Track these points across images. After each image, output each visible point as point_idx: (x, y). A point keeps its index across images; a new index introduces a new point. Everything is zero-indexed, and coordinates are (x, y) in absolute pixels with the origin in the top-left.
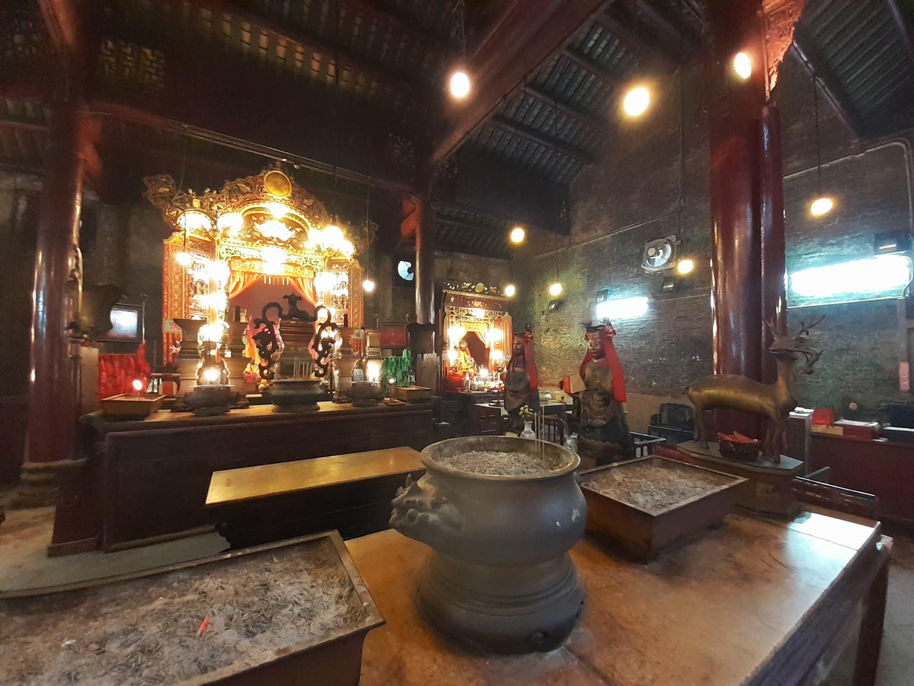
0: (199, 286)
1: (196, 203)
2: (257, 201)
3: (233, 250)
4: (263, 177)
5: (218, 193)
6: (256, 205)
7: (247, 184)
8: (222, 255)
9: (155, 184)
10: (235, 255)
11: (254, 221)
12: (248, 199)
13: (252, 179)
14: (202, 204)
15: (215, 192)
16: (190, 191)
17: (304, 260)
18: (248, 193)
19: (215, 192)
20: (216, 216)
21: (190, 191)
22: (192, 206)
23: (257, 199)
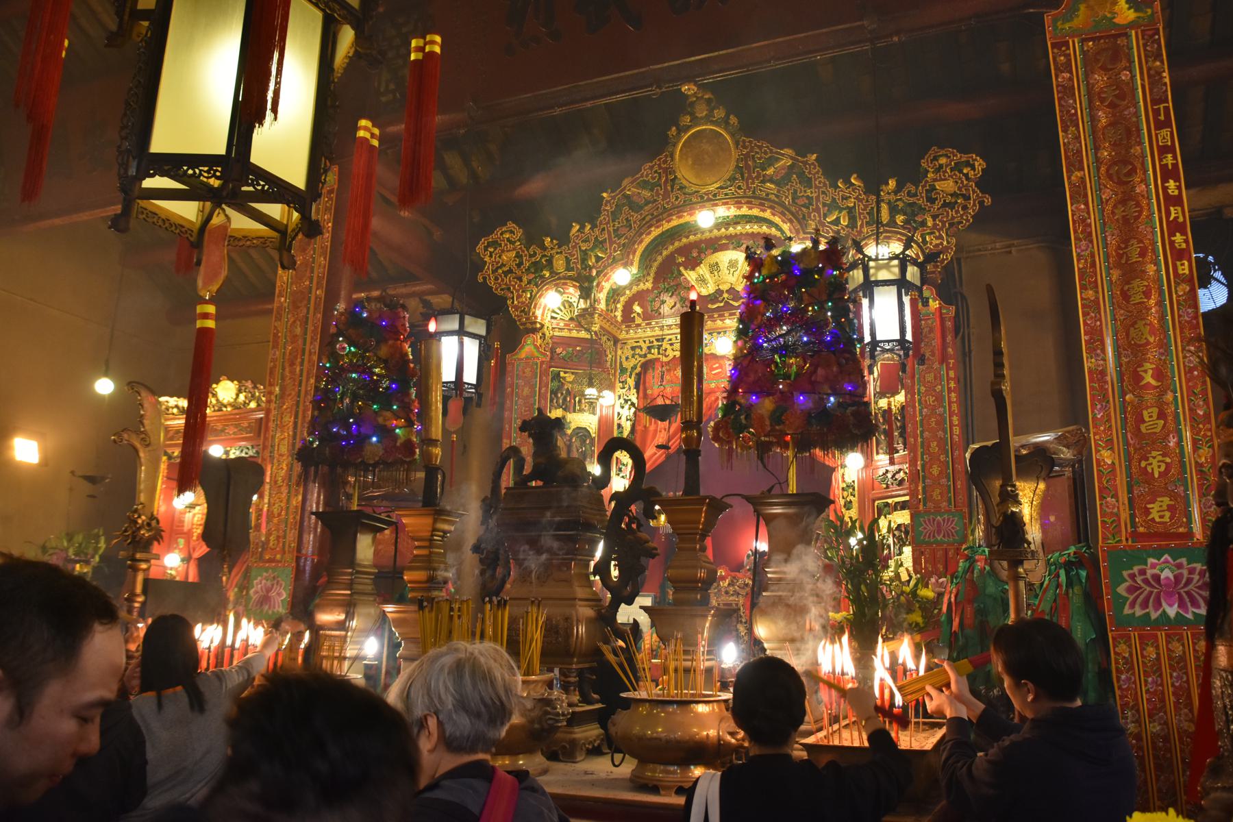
1: (559, 264)
3: (644, 346)
4: (672, 156)
7: (645, 185)
8: (625, 364)
9: (495, 249)
10: (650, 357)
12: (647, 219)
13: (651, 167)
14: (568, 261)
15: (588, 227)
18: (646, 204)
19: (588, 227)
22: (553, 273)
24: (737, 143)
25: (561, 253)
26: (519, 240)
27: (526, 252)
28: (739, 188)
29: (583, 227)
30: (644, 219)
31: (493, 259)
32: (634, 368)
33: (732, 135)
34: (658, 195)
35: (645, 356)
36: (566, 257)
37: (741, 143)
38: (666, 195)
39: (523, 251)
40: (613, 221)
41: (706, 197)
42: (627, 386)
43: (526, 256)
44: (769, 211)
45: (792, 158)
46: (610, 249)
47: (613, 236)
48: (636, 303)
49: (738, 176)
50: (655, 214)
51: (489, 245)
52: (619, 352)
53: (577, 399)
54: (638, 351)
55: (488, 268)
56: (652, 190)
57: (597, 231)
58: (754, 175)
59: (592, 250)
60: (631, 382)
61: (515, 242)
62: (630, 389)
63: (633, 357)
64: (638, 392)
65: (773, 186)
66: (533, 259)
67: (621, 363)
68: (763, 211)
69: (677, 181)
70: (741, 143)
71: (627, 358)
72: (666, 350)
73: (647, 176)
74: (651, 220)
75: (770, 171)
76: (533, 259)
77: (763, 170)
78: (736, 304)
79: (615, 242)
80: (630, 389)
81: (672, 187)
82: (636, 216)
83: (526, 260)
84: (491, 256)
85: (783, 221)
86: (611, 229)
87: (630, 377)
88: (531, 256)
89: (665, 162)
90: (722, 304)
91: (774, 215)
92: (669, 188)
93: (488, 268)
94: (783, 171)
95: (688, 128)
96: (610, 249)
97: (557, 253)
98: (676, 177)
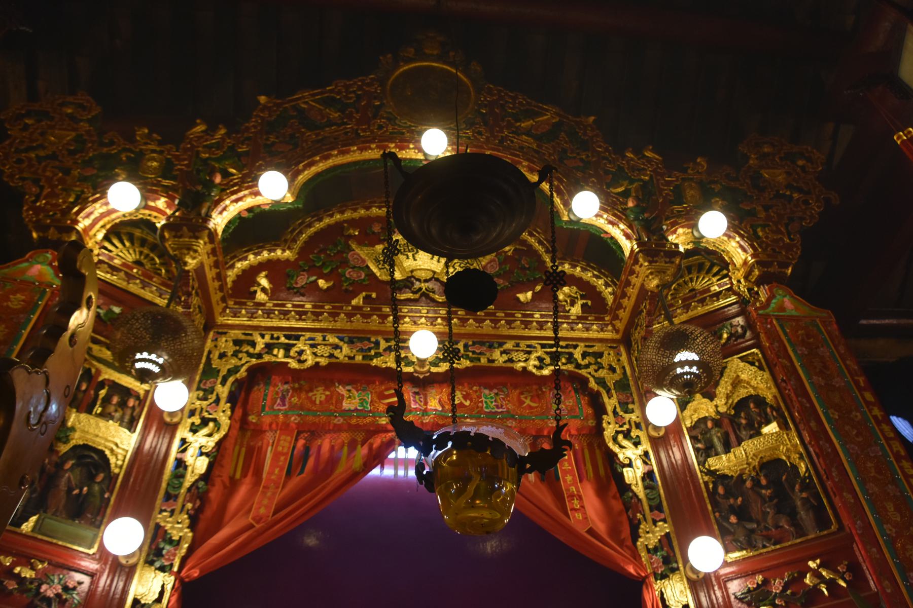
10: (267, 358)
11: (350, 237)
32: (235, 370)
35: (259, 356)
42: (213, 397)
48: (264, 274)
52: (209, 344)
53: (103, 393)
54: (246, 348)
60: (223, 391)
62: (217, 401)
63: (235, 354)
64: (233, 409)
67: (209, 359)
71: (222, 356)
72: (301, 353)
77: (517, 121)
80: (217, 401)
87: (223, 383)
90: (417, 296)
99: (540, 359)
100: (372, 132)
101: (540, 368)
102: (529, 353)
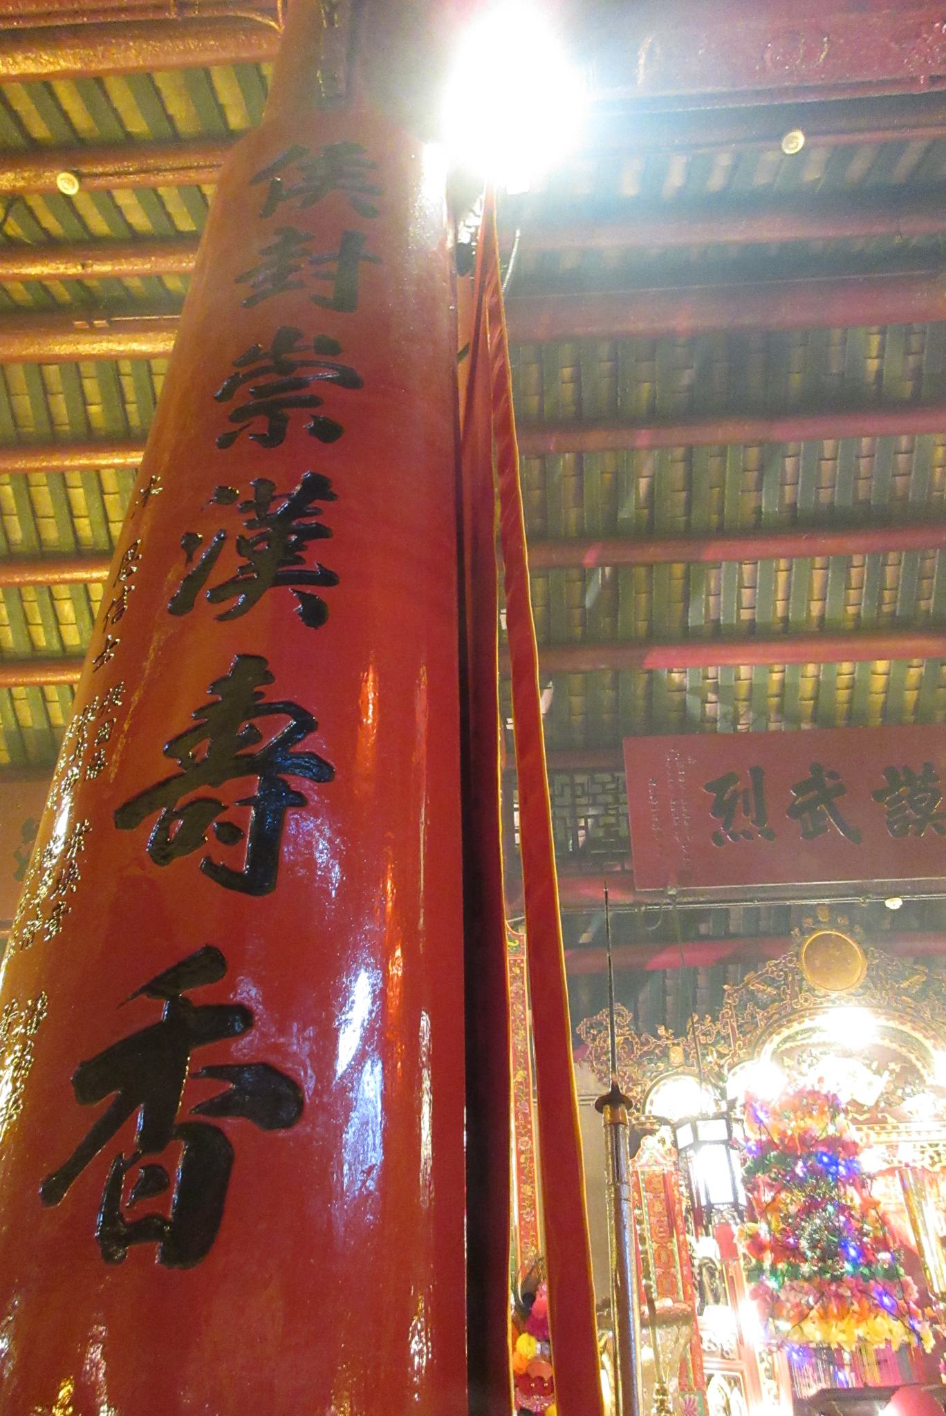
0: (706, 1279)
1: (676, 1055)
2: (796, 1016)
4: (797, 955)
5: (714, 1021)
6: (796, 1027)
7: (772, 982)
9: (600, 1032)
12: (776, 1017)
13: (776, 965)
16: (661, 1031)
17: (930, 1151)
18: (773, 1002)
20: (720, 1077)
21: (661, 1031)
23: (794, 1011)
24: (865, 953)
25: (678, 1044)
26: (628, 1025)
27: (637, 1040)
28: (873, 997)
29: (702, 1019)
30: (770, 1018)
31: (597, 1043)
33: (859, 943)
34: (785, 994)
36: (684, 1050)
37: (870, 953)
38: (794, 996)
39: (634, 1038)
40: (737, 1015)
41: (838, 1002)
43: (637, 1043)
44: (909, 1024)
45: (926, 974)
46: (735, 1046)
47: (737, 1032)
49: (871, 985)
50: (783, 1013)
51: (592, 1027)
55: (591, 1053)
56: (778, 988)
57: (719, 1026)
58: (888, 987)
59: (714, 1045)
61: (624, 1027)
65: (910, 1000)
66: (646, 1048)
68: (902, 1024)
69: (804, 983)
70: (870, 953)
73: (773, 972)
74: (780, 1019)
75: (905, 985)
76: (646, 1048)
78: (861, 1118)
79: (739, 1039)
81: (801, 989)
82: (760, 1015)
83: (637, 1048)
84: (594, 1039)
85: (925, 1036)
86: (735, 1025)
88: (643, 1044)
89: (791, 961)
91: (914, 1029)
92: (797, 989)
93: (591, 1053)
94: (917, 987)
95: (813, 930)
96: (735, 1046)
97: (674, 1044)
98: (803, 979)
99: (932, 1158)
100: (801, 1004)
101: (933, 1164)
102: (923, 1152)
